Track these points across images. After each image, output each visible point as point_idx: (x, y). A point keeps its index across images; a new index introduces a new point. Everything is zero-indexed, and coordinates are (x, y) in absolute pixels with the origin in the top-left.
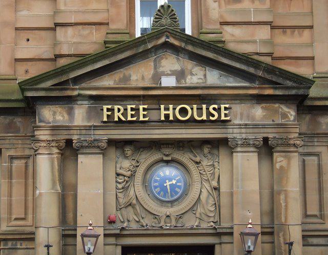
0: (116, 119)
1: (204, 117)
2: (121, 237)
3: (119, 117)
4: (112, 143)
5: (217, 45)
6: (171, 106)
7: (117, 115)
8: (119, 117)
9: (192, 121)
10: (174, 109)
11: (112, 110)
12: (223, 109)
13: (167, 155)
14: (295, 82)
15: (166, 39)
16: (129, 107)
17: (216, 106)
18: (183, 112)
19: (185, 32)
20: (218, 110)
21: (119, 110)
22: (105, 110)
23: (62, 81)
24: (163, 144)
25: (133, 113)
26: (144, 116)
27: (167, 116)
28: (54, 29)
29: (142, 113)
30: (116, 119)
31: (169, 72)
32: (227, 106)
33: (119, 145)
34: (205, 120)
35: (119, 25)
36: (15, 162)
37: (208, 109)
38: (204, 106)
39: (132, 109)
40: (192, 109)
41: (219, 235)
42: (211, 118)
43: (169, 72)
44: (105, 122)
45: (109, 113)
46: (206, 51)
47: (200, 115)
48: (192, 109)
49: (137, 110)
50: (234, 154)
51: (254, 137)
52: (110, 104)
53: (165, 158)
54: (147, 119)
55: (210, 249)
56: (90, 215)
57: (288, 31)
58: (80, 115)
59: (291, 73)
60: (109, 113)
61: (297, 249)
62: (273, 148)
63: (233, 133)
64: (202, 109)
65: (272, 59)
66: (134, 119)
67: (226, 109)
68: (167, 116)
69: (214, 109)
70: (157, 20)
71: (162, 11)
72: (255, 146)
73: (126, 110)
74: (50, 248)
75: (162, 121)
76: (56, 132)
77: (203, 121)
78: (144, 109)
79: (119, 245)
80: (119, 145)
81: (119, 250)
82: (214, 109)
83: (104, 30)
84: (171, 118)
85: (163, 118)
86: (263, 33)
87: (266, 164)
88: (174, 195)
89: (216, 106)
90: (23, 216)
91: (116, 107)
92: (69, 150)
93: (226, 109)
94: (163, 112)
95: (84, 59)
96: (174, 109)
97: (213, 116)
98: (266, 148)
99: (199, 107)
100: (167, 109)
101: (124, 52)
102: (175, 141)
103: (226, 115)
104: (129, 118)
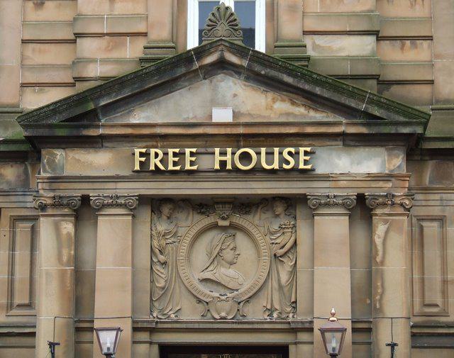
0: (152, 168)
1: (276, 166)
2: (161, 332)
3: (156, 166)
4: (144, 200)
5: (292, 63)
6: (229, 150)
7: (154, 162)
8: (156, 166)
9: (257, 170)
10: (233, 154)
11: (146, 155)
12: (302, 154)
13: (223, 219)
14: (405, 116)
15: (228, 50)
16: (171, 151)
17: (293, 150)
18: (245, 157)
19: (254, 47)
20: (295, 155)
21: (157, 155)
22: (137, 154)
23: (79, 118)
24: (218, 203)
25: (176, 159)
26: (192, 163)
27: (223, 164)
28: (74, 42)
29: (188, 158)
30: (152, 168)
31: (230, 101)
32: (308, 149)
33: (156, 204)
34: (277, 170)
35: (161, 33)
36: (20, 225)
37: (281, 153)
38: (276, 150)
39: (175, 155)
40: (258, 154)
41: (294, 331)
42: (285, 166)
43: (230, 101)
44: (137, 171)
45: (143, 159)
46: (282, 72)
47: (270, 162)
48: (258, 154)
49: (182, 154)
50: (100, 218)
51: (346, 194)
52: (144, 148)
53: (221, 223)
54: (195, 168)
55: (283, 350)
56: (113, 303)
57: (408, 42)
58: (98, 161)
59: (48, 106)
60: (143, 159)
61: (402, 350)
62: (372, 210)
63: (315, 189)
64: (273, 153)
65: (378, 84)
66: (178, 168)
67: (306, 153)
68: (223, 164)
69: (290, 153)
70: (210, 28)
71: (217, 15)
72: (344, 205)
73: (166, 154)
74: (56, 346)
75: (217, 171)
76: (55, 186)
77: (273, 171)
78: (192, 154)
79: (155, 343)
80: (156, 204)
81: (155, 351)
82: (290, 153)
83: (141, 43)
84: (229, 167)
85: (217, 167)
86: (359, 46)
87: (361, 233)
88: (225, 275)
89: (293, 150)
90: (27, 301)
91: (153, 151)
92: (84, 211)
93: (306, 153)
94: (218, 158)
95: (110, 84)
96: (233, 154)
97: (288, 163)
98: (362, 208)
99: (269, 151)
100: (223, 154)
101: (166, 71)
102: (235, 198)
103: (306, 162)
104: (171, 167)
